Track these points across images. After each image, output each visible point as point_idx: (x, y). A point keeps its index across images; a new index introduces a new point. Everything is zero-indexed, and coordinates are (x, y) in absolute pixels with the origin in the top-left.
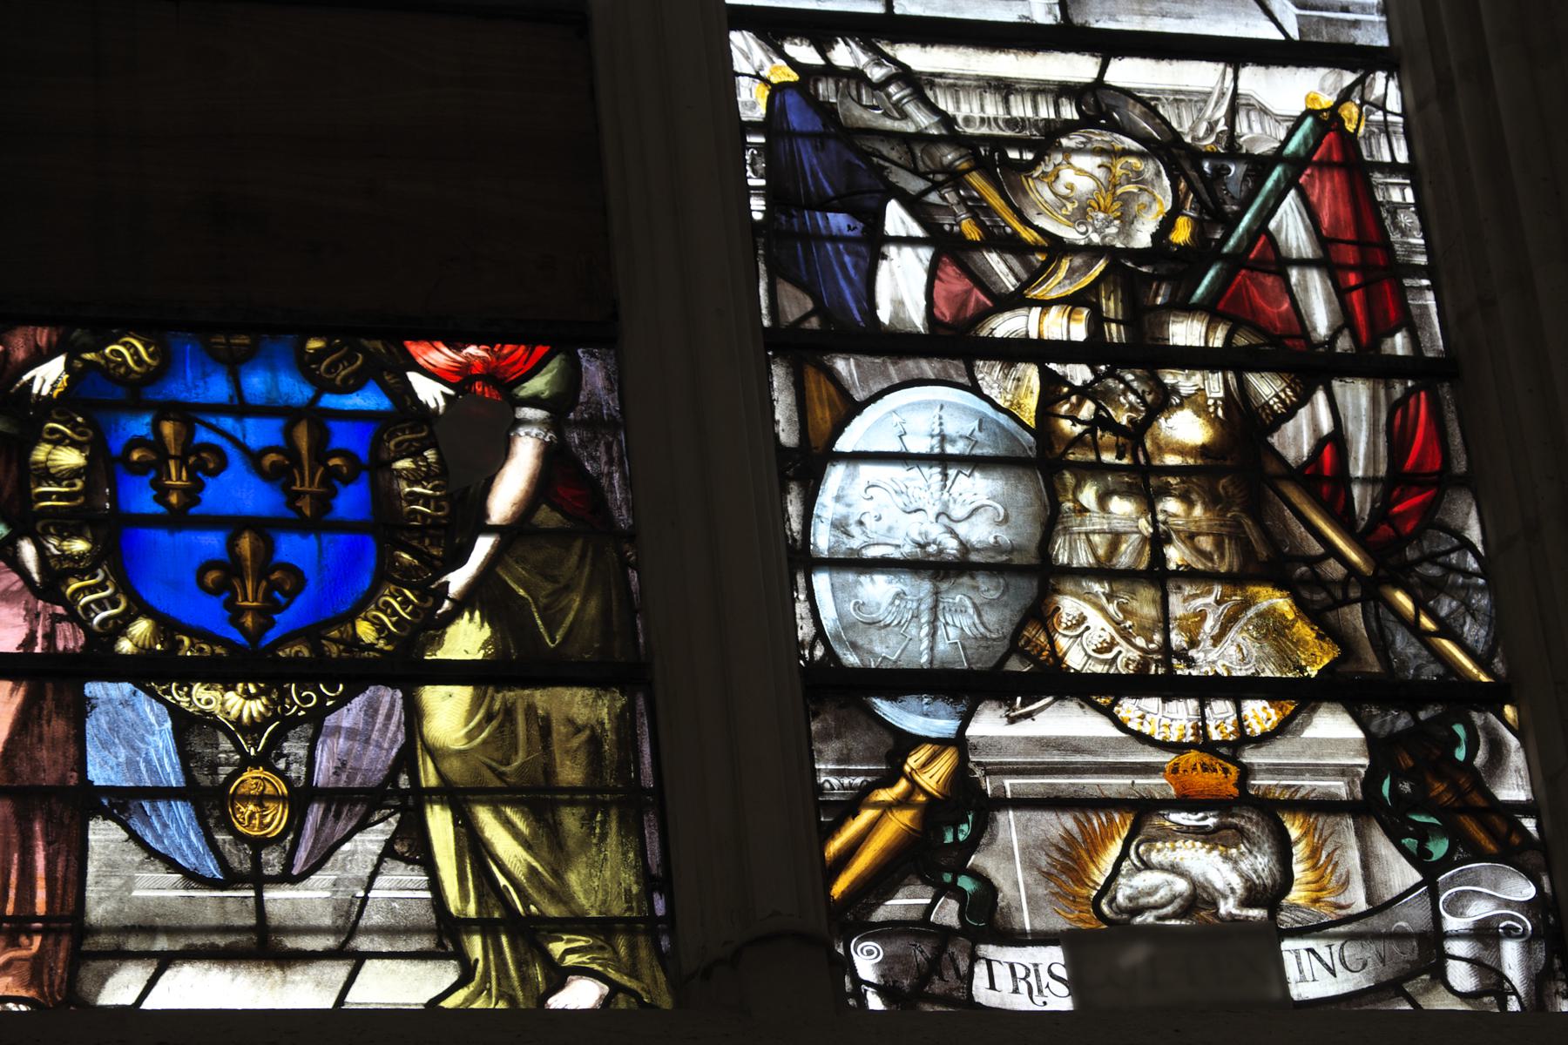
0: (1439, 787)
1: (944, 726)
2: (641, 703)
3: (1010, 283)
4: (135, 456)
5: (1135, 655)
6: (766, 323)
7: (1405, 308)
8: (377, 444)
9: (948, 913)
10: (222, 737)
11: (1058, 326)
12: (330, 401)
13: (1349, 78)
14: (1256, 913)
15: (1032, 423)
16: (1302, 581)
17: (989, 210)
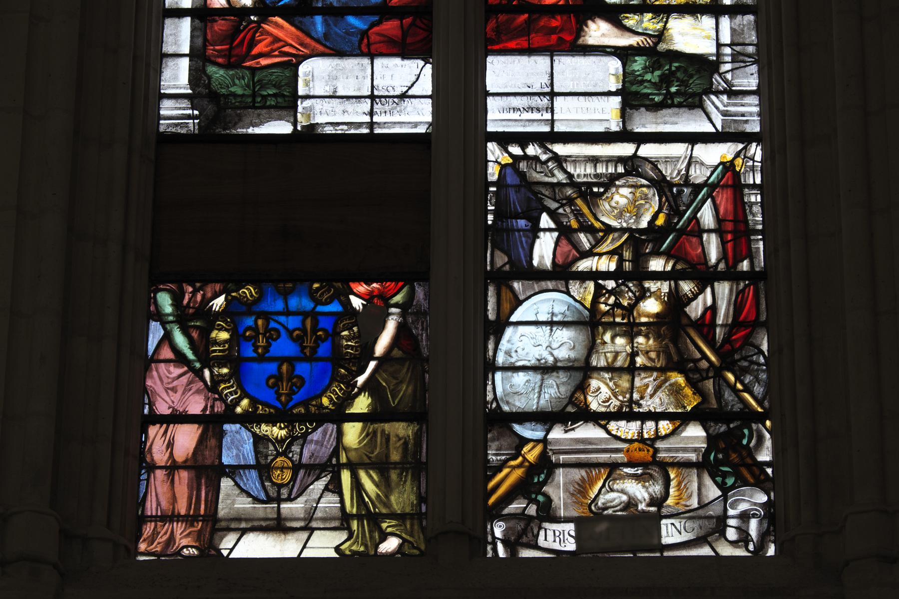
0: (734, 456)
1: (539, 434)
2: (424, 427)
3: (587, 246)
4: (248, 334)
5: (618, 403)
6: (488, 268)
7: (749, 248)
8: (336, 325)
9: (532, 510)
10: (270, 445)
11: (607, 264)
12: (320, 308)
13: (741, 146)
14: (653, 509)
15: (588, 306)
16: (691, 370)
17: (583, 215)
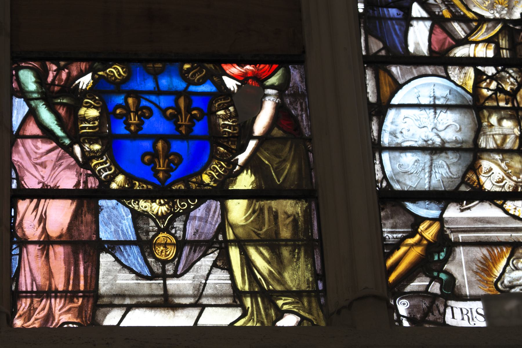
1: (434, 213)
2: (313, 205)
3: (462, 35)
4: (118, 111)
5: (513, 184)
6: (364, 53)
9: (436, 288)
10: (151, 221)
12: (192, 88)
15: (470, 91)
